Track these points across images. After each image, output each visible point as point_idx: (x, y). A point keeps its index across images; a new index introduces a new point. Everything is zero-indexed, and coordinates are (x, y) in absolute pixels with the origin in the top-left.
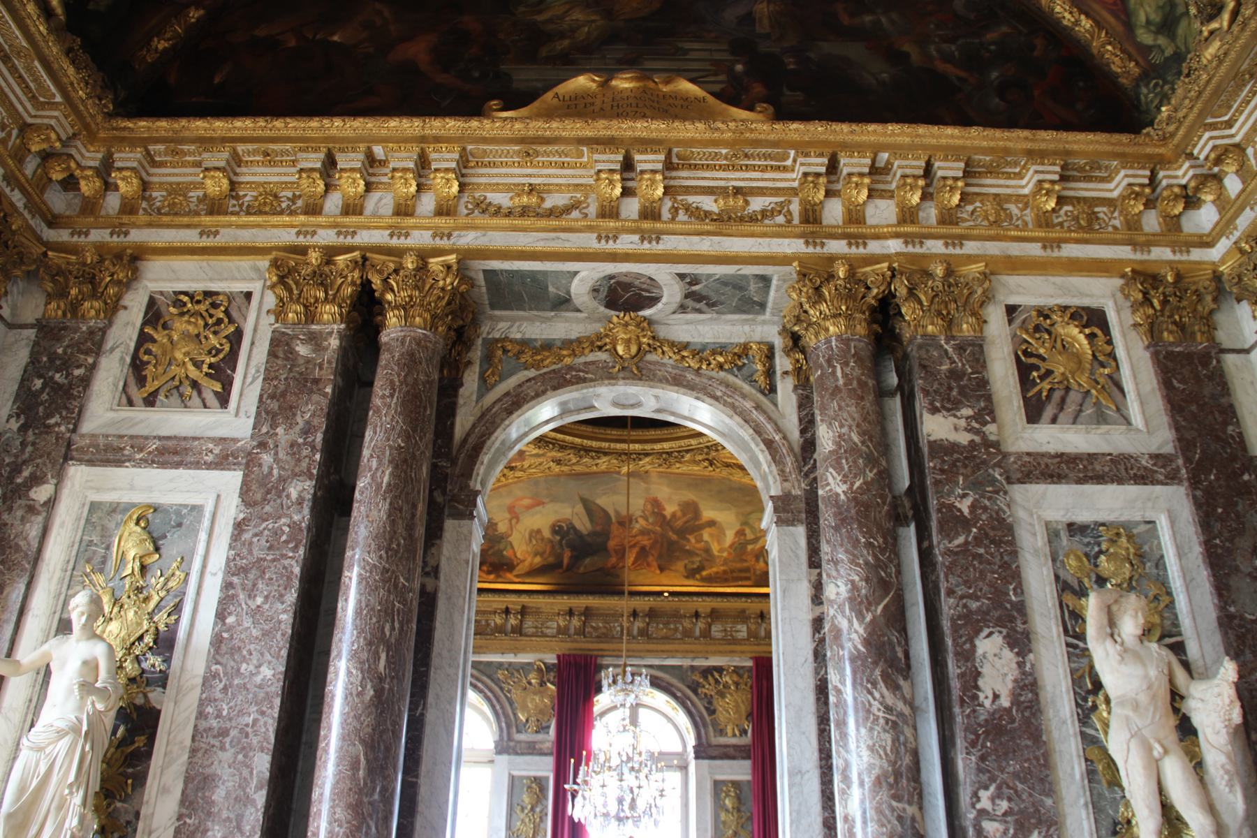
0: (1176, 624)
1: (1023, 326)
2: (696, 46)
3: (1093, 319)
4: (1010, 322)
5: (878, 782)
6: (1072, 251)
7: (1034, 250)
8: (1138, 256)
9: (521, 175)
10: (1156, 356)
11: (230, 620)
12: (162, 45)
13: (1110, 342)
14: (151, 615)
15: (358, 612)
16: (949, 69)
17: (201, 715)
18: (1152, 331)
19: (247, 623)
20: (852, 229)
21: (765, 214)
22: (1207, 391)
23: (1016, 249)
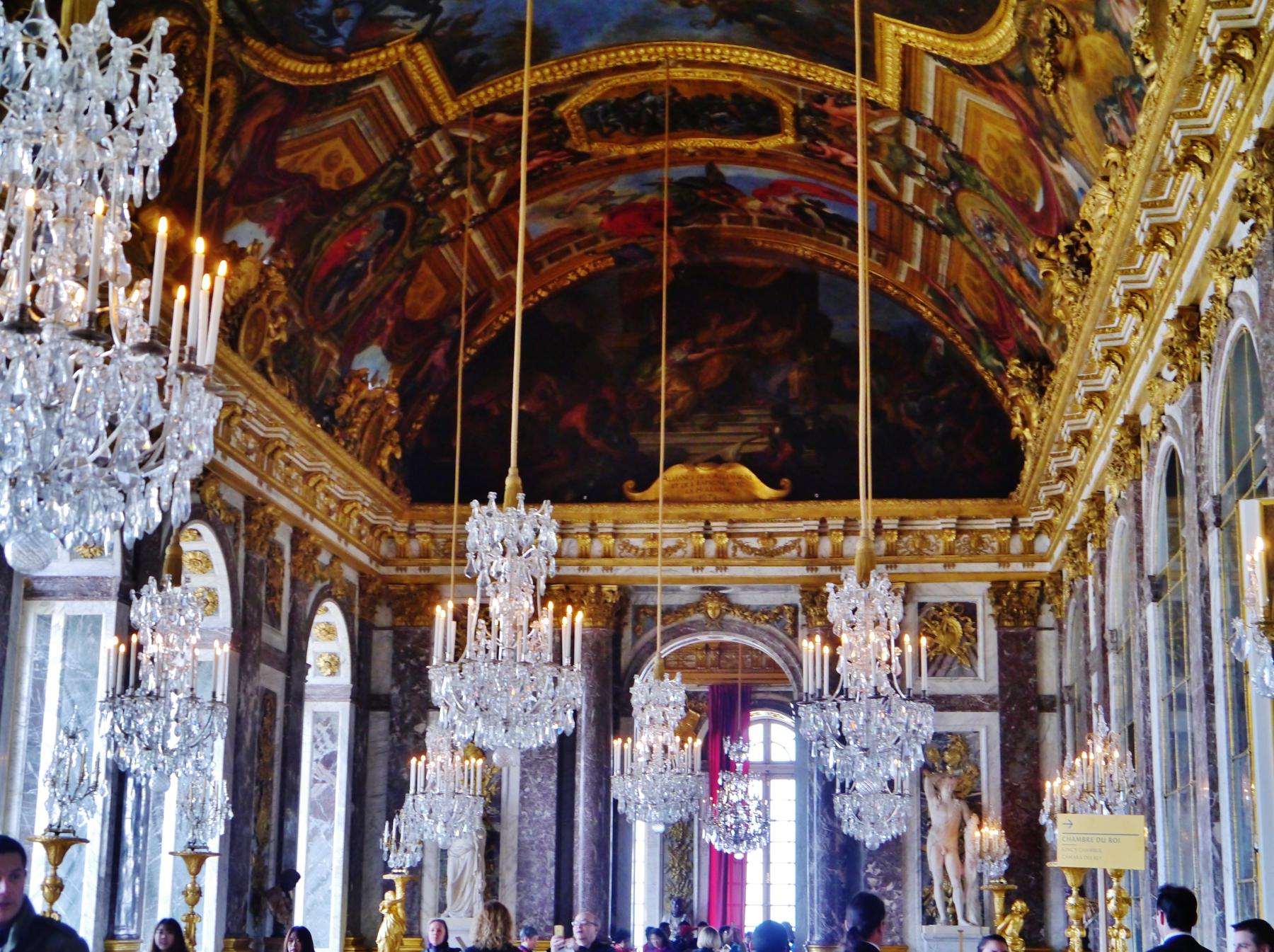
0: (979, 787)
1: (926, 618)
2: (751, 412)
3: (967, 611)
4: (919, 613)
5: (823, 859)
6: (962, 567)
7: (939, 568)
8: (1002, 570)
9: (647, 528)
10: (999, 634)
11: (527, 790)
12: (419, 426)
13: (975, 626)
14: (487, 787)
15: (586, 784)
16: (912, 425)
17: (520, 835)
18: (999, 619)
19: (535, 791)
20: (834, 560)
21: (786, 548)
22: (1023, 657)
23: (927, 568)
